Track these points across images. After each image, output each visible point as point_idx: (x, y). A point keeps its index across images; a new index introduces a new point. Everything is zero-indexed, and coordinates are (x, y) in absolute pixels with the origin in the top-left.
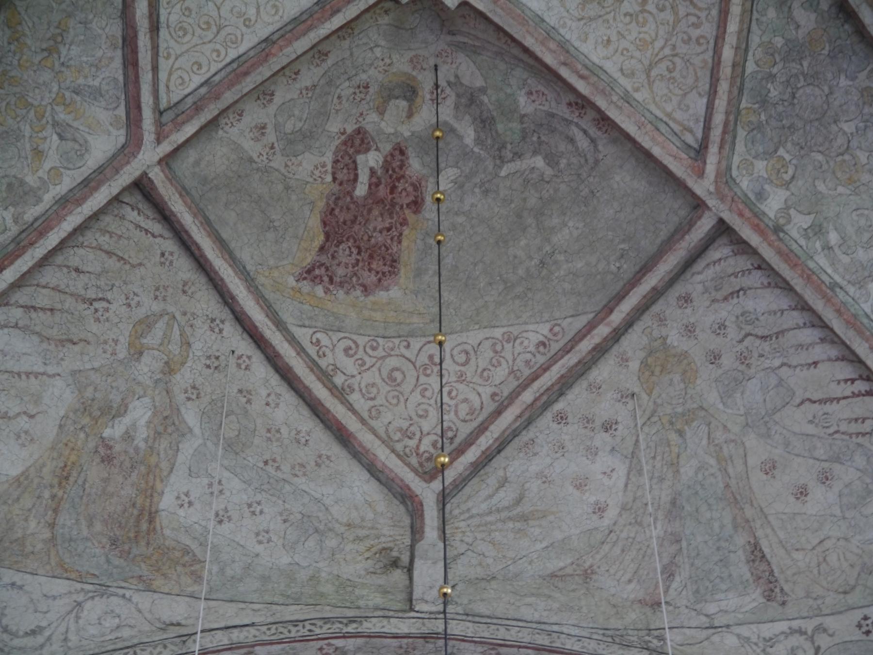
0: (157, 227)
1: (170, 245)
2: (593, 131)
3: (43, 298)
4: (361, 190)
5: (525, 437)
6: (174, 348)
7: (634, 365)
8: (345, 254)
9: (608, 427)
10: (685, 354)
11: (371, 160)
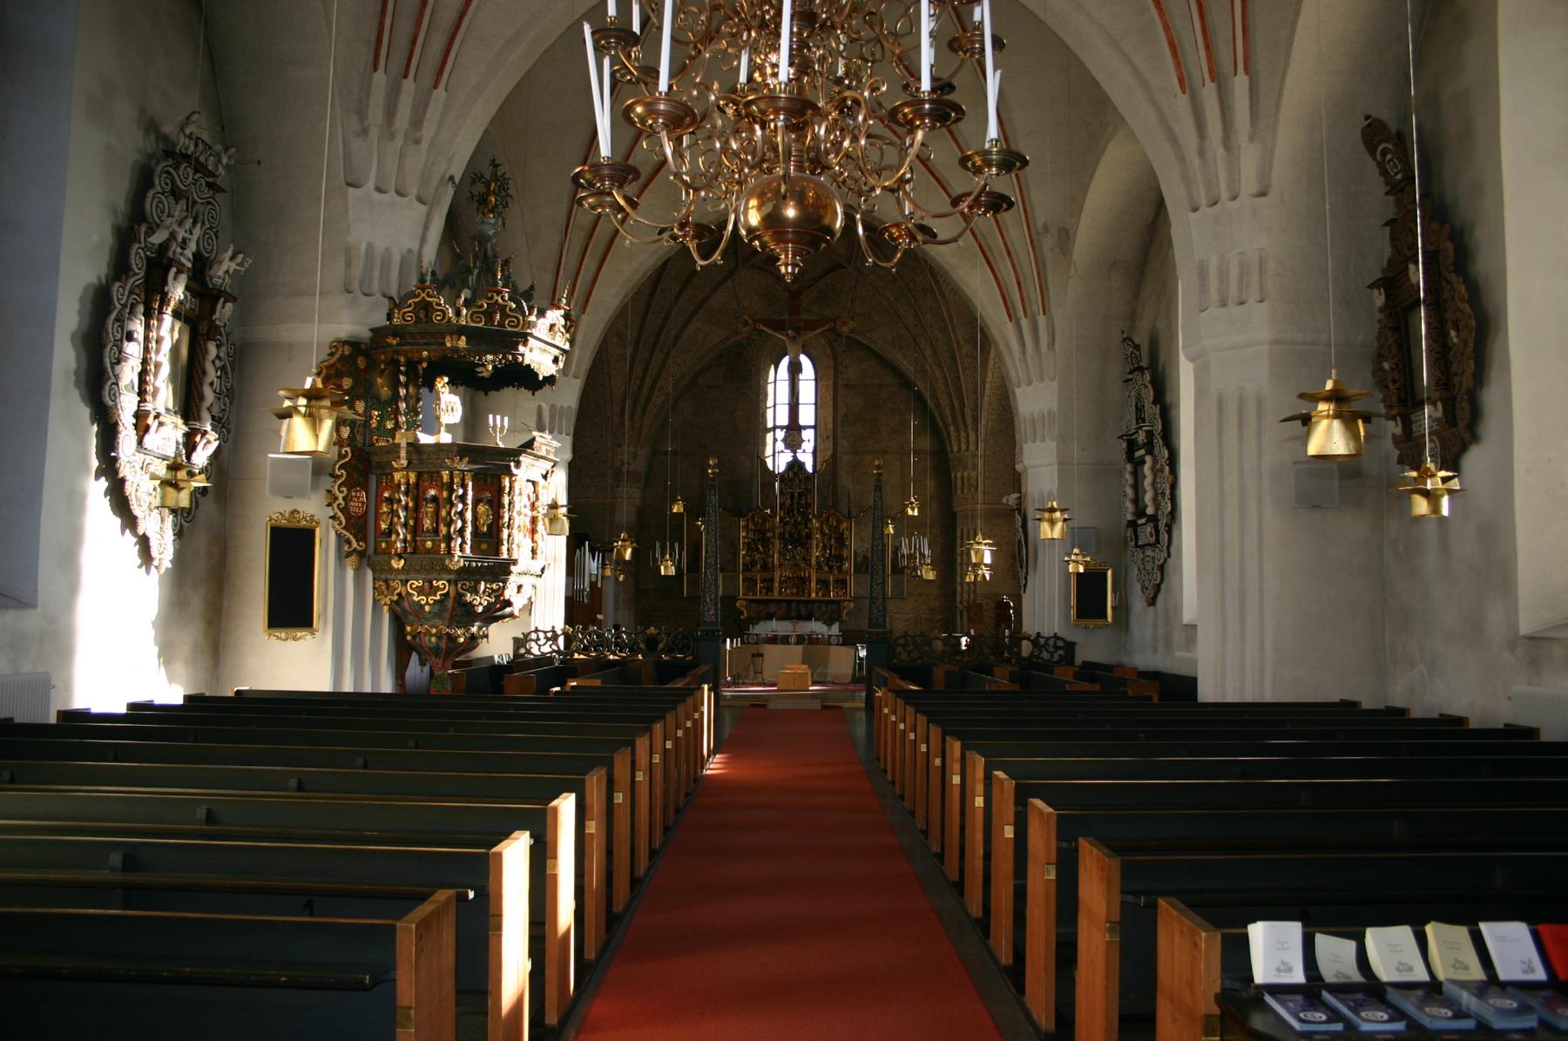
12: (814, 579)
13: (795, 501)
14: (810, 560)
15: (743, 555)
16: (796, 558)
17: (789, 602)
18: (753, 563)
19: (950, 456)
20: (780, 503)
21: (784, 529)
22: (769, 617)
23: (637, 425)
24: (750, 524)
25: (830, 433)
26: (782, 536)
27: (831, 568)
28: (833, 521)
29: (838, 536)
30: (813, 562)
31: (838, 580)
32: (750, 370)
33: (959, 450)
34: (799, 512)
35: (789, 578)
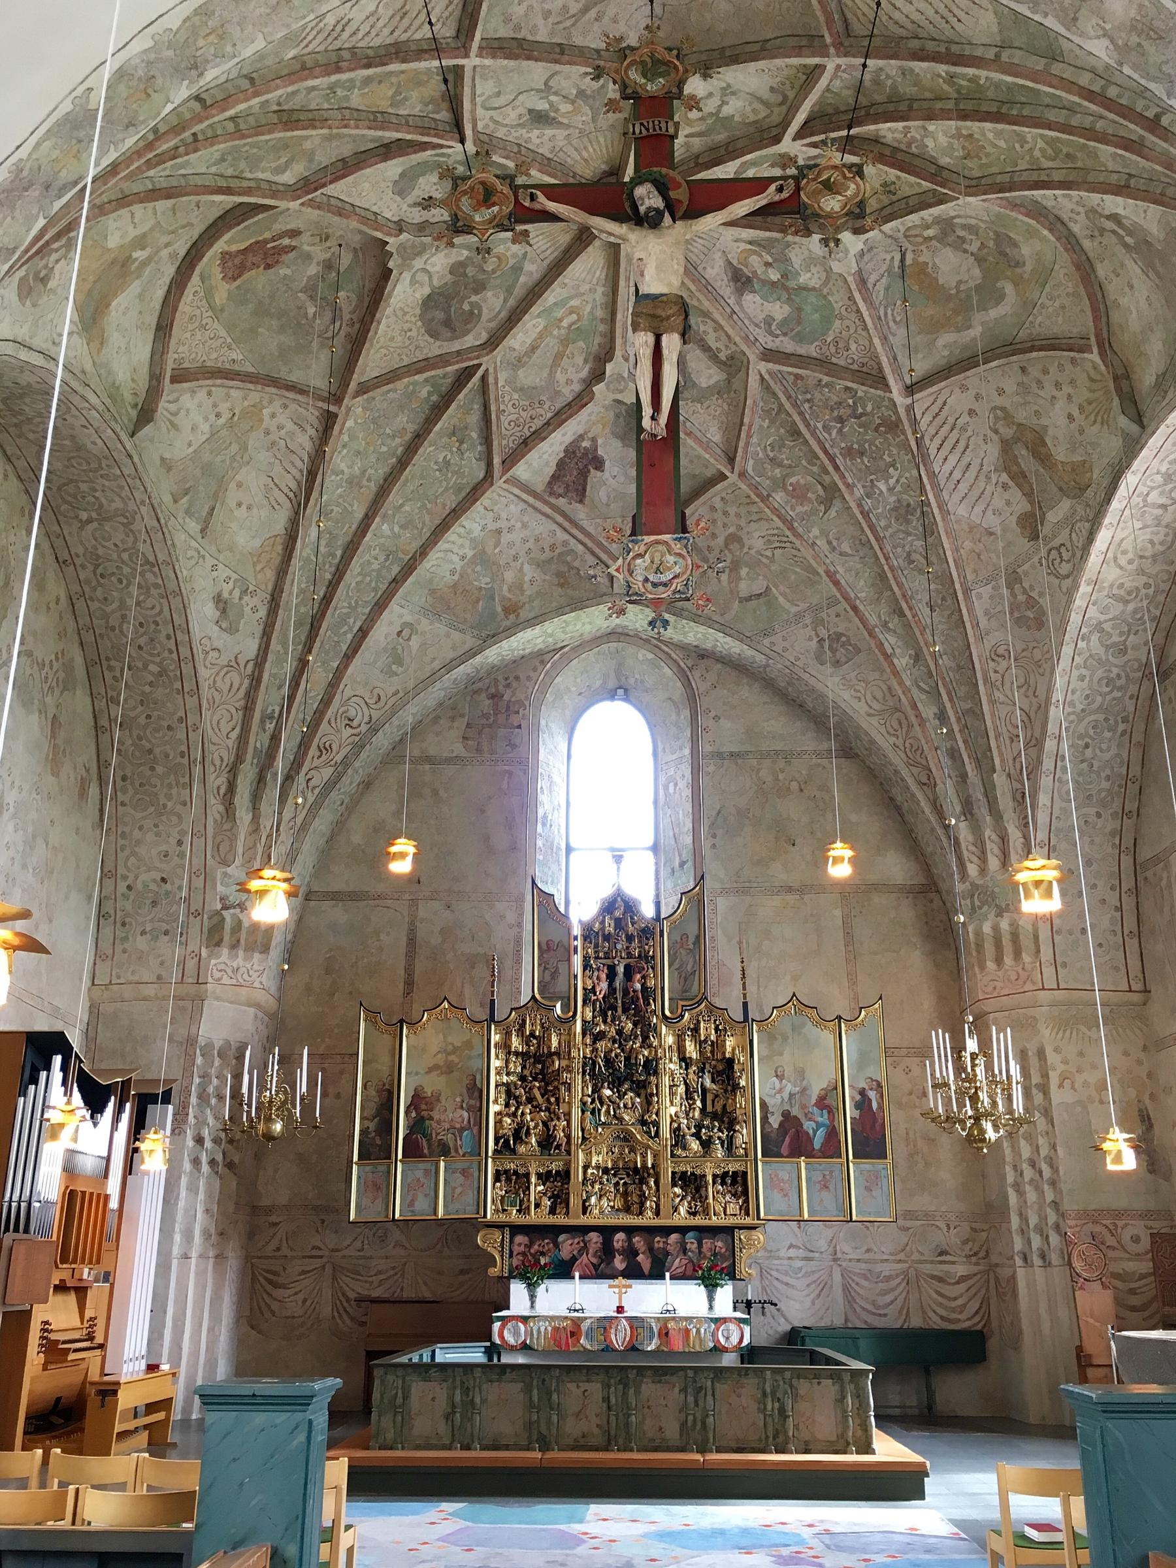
2: (342, 333)
9: (218, 415)
10: (261, 421)
11: (286, 241)
12: (668, 1169)
13: (618, 982)
14: (656, 1124)
15: (497, 1114)
16: (621, 1120)
17: (607, 1232)
18: (519, 1134)
19: (959, 887)
20: (584, 989)
21: (594, 1050)
22: (563, 1271)
23: (267, 823)
24: (514, 1038)
25: (687, 855)
26: (589, 1065)
27: (706, 1144)
28: (707, 1030)
29: (720, 1067)
30: (666, 1132)
31: (725, 1174)
32: (519, 727)
33: (983, 871)
34: (625, 1010)
35: (606, 1171)
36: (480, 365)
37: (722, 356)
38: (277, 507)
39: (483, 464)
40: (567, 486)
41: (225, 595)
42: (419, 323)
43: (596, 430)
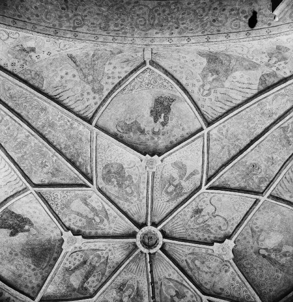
0: (205, 113)
1: (202, 109)
2: (118, 132)
3: (229, 103)
4: (163, 115)
5: (127, 74)
6: (202, 90)
7: (105, 89)
8: (166, 104)
11: (162, 120)
36: (92, 184)
37: (86, 285)
38: (55, 89)
39: (40, 183)
40: (5, 220)
41: (32, 54)
42: (113, 162)
43: (33, 231)
